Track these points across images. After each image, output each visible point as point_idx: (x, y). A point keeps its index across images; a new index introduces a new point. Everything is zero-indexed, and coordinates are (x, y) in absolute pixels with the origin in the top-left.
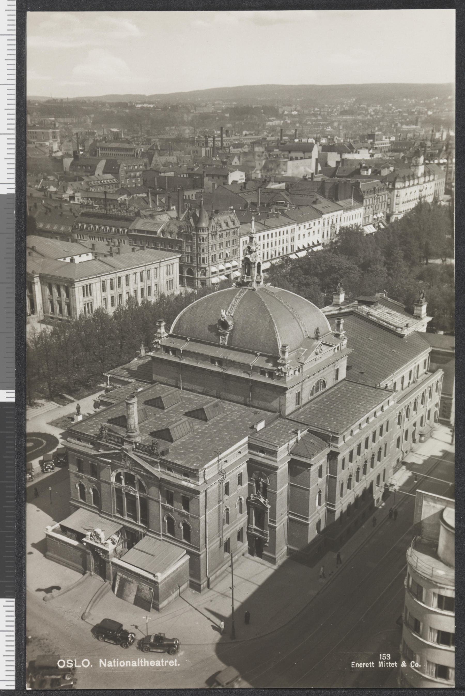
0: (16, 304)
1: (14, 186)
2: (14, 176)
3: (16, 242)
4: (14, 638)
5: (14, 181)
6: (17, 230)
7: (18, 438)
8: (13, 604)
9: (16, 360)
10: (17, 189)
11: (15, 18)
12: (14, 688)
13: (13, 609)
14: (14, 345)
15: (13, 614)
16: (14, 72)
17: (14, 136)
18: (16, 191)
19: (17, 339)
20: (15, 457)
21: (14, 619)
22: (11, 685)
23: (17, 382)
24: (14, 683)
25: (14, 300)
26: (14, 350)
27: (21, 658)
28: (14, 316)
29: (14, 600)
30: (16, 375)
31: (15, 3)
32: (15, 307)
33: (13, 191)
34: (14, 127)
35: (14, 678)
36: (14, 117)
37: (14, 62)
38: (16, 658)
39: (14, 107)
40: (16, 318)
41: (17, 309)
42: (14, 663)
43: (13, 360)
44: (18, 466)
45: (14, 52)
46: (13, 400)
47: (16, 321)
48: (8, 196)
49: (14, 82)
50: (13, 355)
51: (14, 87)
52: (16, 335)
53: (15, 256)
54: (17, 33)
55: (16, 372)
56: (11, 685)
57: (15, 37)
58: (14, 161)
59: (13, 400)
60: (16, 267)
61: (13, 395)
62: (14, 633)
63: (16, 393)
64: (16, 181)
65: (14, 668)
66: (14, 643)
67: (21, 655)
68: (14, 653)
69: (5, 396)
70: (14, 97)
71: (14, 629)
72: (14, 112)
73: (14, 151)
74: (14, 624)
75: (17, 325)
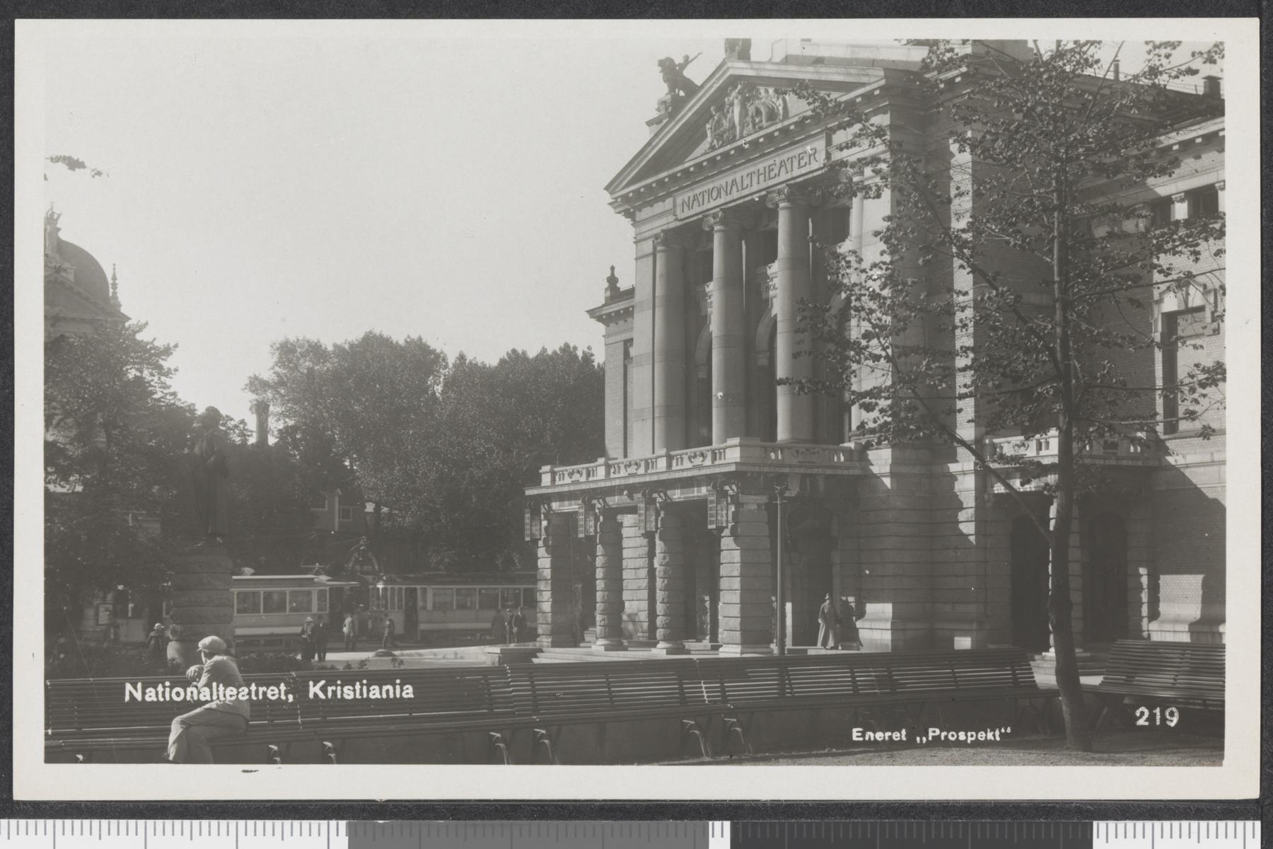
1: (333, 823)
2: (315, 823)
4: (1167, 824)
5: (324, 823)
6: (414, 818)
8: (1102, 824)
9: (653, 819)
10: (339, 816)
11: (23, 822)
12: (1258, 824)
13: (1112, 824)
14: (625, 824)
15: (1121, 824)
17: (242, 823)
18: (342, 818)
19: (614, 818)
20: (830, 820)
21: (1130, 824)
22: (1253, 828)
23: (693, 818)
24: (1249, 823)
26: (635, 823)
27: (1202, 811)
28: (572, 824)
29: (1095, 823)
30: (682, 819)
31: (4, 822)
32: (555, 822)
33: (343, 824)
34: (223, 823)
35: (1240, 824)
36: (205, 823)
38: (1203, 819)
39: (187, 822)
40: (577, 818)
41: (561, 817)
42: (1213, 823)
43: (653, 824)
44: (849, 816)
46: (727, 824)
48: (351, 833)
51: (150, 822)
53: (462, 822)
54: (51, 817)
55: (675, 818)
56: (1253, 828)
57: (59, 822)
58: (287, 823)
59: (727, 824)
60: (483, 819)
61: (718, 824)
62: (1157, 824)
65: (1222, 824)
66: (1176, 824)
68: (1194, 824)
70: (168, 822)
71: (1148, 824)
72: (196, 823)
74: (1139, 824)
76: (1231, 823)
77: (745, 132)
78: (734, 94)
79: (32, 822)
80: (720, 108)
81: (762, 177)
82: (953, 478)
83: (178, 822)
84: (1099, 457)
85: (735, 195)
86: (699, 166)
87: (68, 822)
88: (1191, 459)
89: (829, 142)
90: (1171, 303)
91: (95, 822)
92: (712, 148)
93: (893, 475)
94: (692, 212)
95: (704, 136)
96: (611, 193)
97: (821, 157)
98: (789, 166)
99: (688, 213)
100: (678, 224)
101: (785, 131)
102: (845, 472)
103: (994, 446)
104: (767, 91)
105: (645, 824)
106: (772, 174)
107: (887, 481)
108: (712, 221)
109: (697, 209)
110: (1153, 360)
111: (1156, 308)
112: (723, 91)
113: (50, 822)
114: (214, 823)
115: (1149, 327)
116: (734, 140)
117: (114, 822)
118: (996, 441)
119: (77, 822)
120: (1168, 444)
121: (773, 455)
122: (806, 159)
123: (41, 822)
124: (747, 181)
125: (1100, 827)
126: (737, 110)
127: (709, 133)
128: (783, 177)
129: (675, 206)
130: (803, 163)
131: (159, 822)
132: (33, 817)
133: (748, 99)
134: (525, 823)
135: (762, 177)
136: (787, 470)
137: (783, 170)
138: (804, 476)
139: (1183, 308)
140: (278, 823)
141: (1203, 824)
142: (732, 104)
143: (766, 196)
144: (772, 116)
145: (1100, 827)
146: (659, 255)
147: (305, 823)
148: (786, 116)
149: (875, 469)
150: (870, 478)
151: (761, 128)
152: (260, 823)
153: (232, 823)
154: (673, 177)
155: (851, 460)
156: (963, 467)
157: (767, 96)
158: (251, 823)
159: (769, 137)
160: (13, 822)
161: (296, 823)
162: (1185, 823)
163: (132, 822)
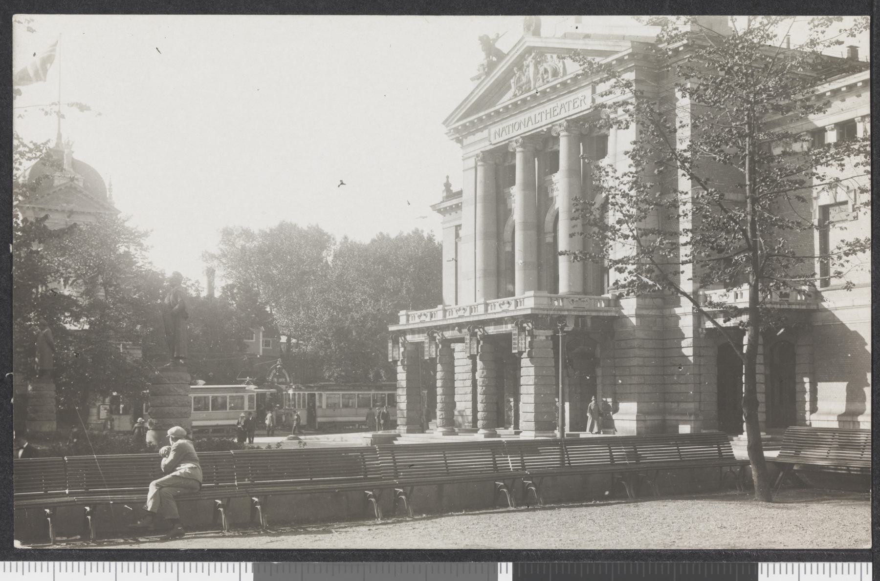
0: (391, 561)
1: (243, 564)
2: (231, 564)
3: (313, 561)
4: (808, 564)
5: (237, 564)
6: (298, 561)
7: (558, 559)
8: (765, 565)
9: (460, 561)
11: (32, 563)
12: (870, 564)
13: (771, 564)
14: (441, 564)
15: (777, 564)
16: (101, 563)
17: (181, 564)
18: (249, 561)
19: (434, 560)
21: (783, 564)
23: (488, 560)
24: (864, 564)
25: (386, 564)
26: (448, 564)
29: (760, 564)
30: (479, 561)
33: (250, 565)
34: (169, 564)
35: (858, 564)
36: (156, 564)
37: (88, 563)
38: (833, 561)
39: (144, 563)
41: (397, 560)
42: (839, 564)
43: (460, 564)
44: (593, 559)
45: (76, 563)
46: (510, 564)
47: (411, 561)
48: (256, 571)
49: (113, 563)
50: (454, 564)
51: (119, 563)
52: (429, 561)
57: (57, 563)
58: (212, 564)
59: (510, 564)
60: (345, 561)
61: (504, 564)
62: (802, 564)
63: (502, 561)
64: (237, 561)
65: (846, 564)
66: (815, 564)
67: (829, 555)
68: (827, 564)
69: (505, 575)
70: (131, 564)
71: (796, 564)
72: (150, 564)
73: (200, 564)
74: (790, 564)
75: (418, 561)
76: (852, 564)
77: (537, 85)
78: (530, 59)
79: (39, 563)
80: (520, 69)
81: (548, 115)
82: (678, 318)
83: (138, 563)
84: (776, 303)
85: (531, 127)
86: (506, 108)
87: (63, 563)
88: (839, 304)
89: (594, 92)
90: (825, 199)
91: (82, 563)
92: (515, 96)
93: (637, 316)
94: (501, 139)
95: (510, 88)
96: (447, 127)
97: (588, 103)
98: (567, 107)
99: (498, 140)
100: (492, 147)
101: (564, 84)
102: (605, 314)
103: (706, 296)
104: (552, 57)
105: (454, 565)
106: (556, 113)
107: (634, 320)
108: (514, 144)
109: (505, 137)
110: (813, 237)
111: (814, 202)
112: (522, 57)
113: (51, 563)
114: (162, 564)
115: (810, 214)
116: (529, 90)
117: (94, 563)
118: (707, 292)
119: (70, 563)
120: (823, 294)
121: (556, 303)
122: (578, 103)
123: (45, 563)
124: (538, 118)
125: (763, 567)
126: (532, 69)
127: (513, 85)
128: (563, 115)
129: (490, 135)
130: (576, 105)
131: (125, 563)
132: (40, 560)
133: (539, 63)
134: (373, 564)
135: (548, 115)
136: (566, 313)
137: (563, 110)
138: (577, 317)
139: (833, 202)
140: (206, 564)
141: (833, 564)
142: (528, 66)
143: (551, 128)
144: (555, 74)
145: (763, 567)
146: (479, 168)
147: (224, 564)
148: (565, 73)
149: (625, 312)
150: (621, 318)
151: (548, 82)
152: (193, 564)
153: (175, 564)
154: (489, 116)
155: (609, 306)
156: (685, 312)
157: (552, 61)
158: (187, 564)
159: (554, 88)
160: (26, 563)
161: (218, 564)
162: (821, 564)
163: (107, 563)
